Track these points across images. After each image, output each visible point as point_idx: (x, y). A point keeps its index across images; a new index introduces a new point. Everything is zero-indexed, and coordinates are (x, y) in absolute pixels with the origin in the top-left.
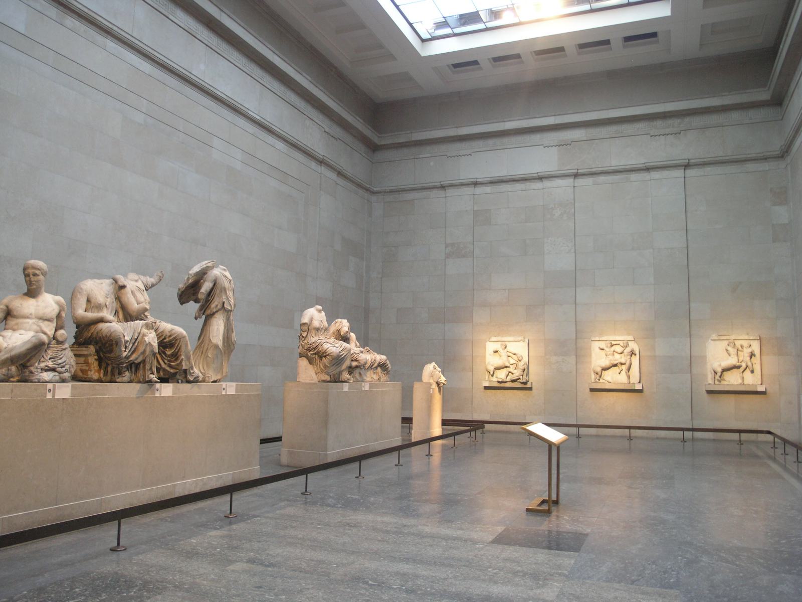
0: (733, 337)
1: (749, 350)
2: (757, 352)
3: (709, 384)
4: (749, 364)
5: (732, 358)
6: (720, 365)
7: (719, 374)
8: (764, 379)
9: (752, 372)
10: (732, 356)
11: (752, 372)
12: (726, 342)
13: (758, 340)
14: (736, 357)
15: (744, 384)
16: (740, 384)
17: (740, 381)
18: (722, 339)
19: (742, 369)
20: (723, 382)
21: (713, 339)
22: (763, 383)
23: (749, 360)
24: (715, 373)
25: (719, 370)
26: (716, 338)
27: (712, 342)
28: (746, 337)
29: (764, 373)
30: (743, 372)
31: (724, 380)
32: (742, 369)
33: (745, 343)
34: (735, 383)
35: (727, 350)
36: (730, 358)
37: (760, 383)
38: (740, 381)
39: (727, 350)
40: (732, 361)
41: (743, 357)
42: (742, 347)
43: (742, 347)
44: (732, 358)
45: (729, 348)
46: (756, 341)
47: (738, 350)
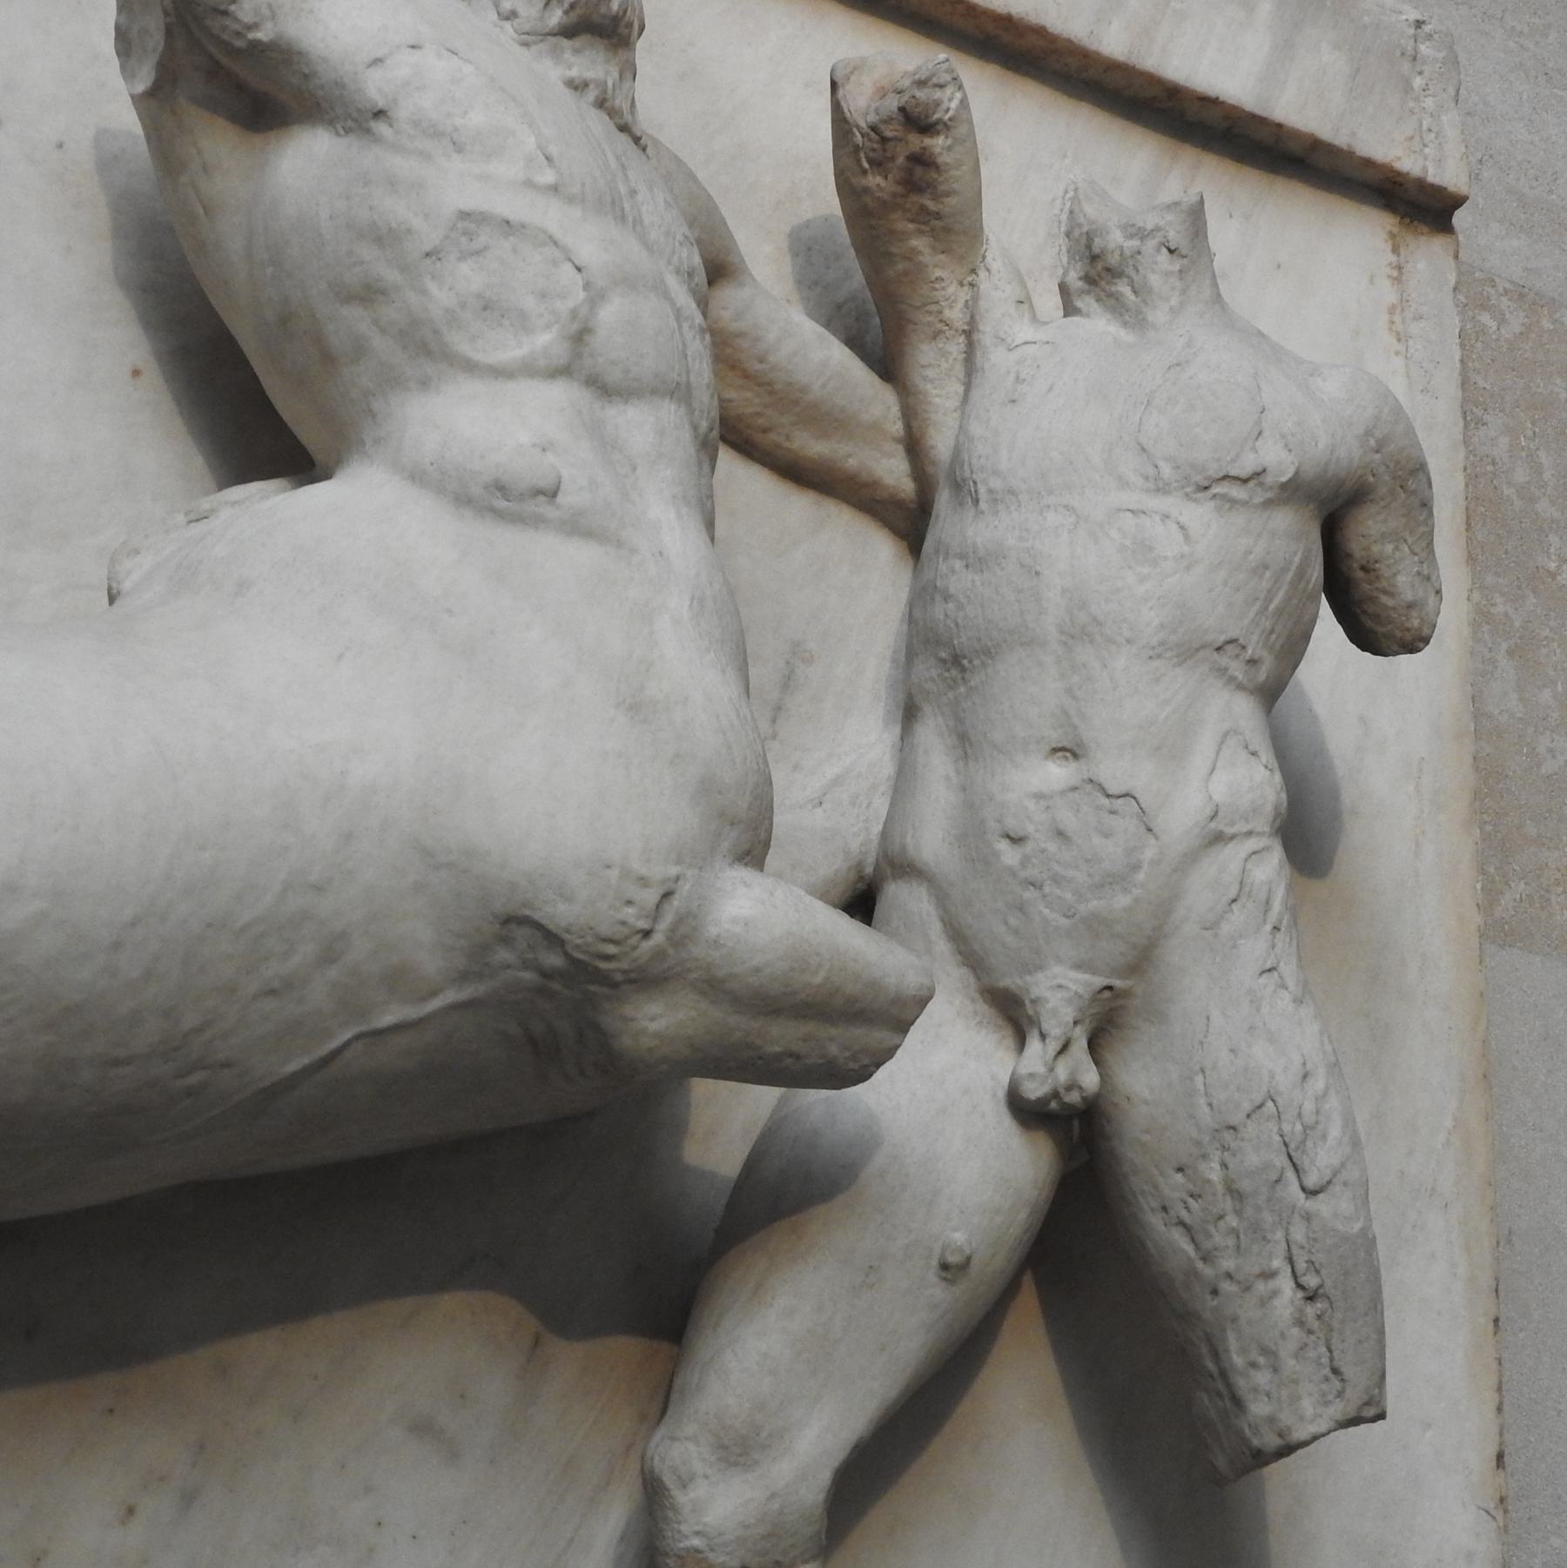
5: (510, 501)
44: (510, 501)
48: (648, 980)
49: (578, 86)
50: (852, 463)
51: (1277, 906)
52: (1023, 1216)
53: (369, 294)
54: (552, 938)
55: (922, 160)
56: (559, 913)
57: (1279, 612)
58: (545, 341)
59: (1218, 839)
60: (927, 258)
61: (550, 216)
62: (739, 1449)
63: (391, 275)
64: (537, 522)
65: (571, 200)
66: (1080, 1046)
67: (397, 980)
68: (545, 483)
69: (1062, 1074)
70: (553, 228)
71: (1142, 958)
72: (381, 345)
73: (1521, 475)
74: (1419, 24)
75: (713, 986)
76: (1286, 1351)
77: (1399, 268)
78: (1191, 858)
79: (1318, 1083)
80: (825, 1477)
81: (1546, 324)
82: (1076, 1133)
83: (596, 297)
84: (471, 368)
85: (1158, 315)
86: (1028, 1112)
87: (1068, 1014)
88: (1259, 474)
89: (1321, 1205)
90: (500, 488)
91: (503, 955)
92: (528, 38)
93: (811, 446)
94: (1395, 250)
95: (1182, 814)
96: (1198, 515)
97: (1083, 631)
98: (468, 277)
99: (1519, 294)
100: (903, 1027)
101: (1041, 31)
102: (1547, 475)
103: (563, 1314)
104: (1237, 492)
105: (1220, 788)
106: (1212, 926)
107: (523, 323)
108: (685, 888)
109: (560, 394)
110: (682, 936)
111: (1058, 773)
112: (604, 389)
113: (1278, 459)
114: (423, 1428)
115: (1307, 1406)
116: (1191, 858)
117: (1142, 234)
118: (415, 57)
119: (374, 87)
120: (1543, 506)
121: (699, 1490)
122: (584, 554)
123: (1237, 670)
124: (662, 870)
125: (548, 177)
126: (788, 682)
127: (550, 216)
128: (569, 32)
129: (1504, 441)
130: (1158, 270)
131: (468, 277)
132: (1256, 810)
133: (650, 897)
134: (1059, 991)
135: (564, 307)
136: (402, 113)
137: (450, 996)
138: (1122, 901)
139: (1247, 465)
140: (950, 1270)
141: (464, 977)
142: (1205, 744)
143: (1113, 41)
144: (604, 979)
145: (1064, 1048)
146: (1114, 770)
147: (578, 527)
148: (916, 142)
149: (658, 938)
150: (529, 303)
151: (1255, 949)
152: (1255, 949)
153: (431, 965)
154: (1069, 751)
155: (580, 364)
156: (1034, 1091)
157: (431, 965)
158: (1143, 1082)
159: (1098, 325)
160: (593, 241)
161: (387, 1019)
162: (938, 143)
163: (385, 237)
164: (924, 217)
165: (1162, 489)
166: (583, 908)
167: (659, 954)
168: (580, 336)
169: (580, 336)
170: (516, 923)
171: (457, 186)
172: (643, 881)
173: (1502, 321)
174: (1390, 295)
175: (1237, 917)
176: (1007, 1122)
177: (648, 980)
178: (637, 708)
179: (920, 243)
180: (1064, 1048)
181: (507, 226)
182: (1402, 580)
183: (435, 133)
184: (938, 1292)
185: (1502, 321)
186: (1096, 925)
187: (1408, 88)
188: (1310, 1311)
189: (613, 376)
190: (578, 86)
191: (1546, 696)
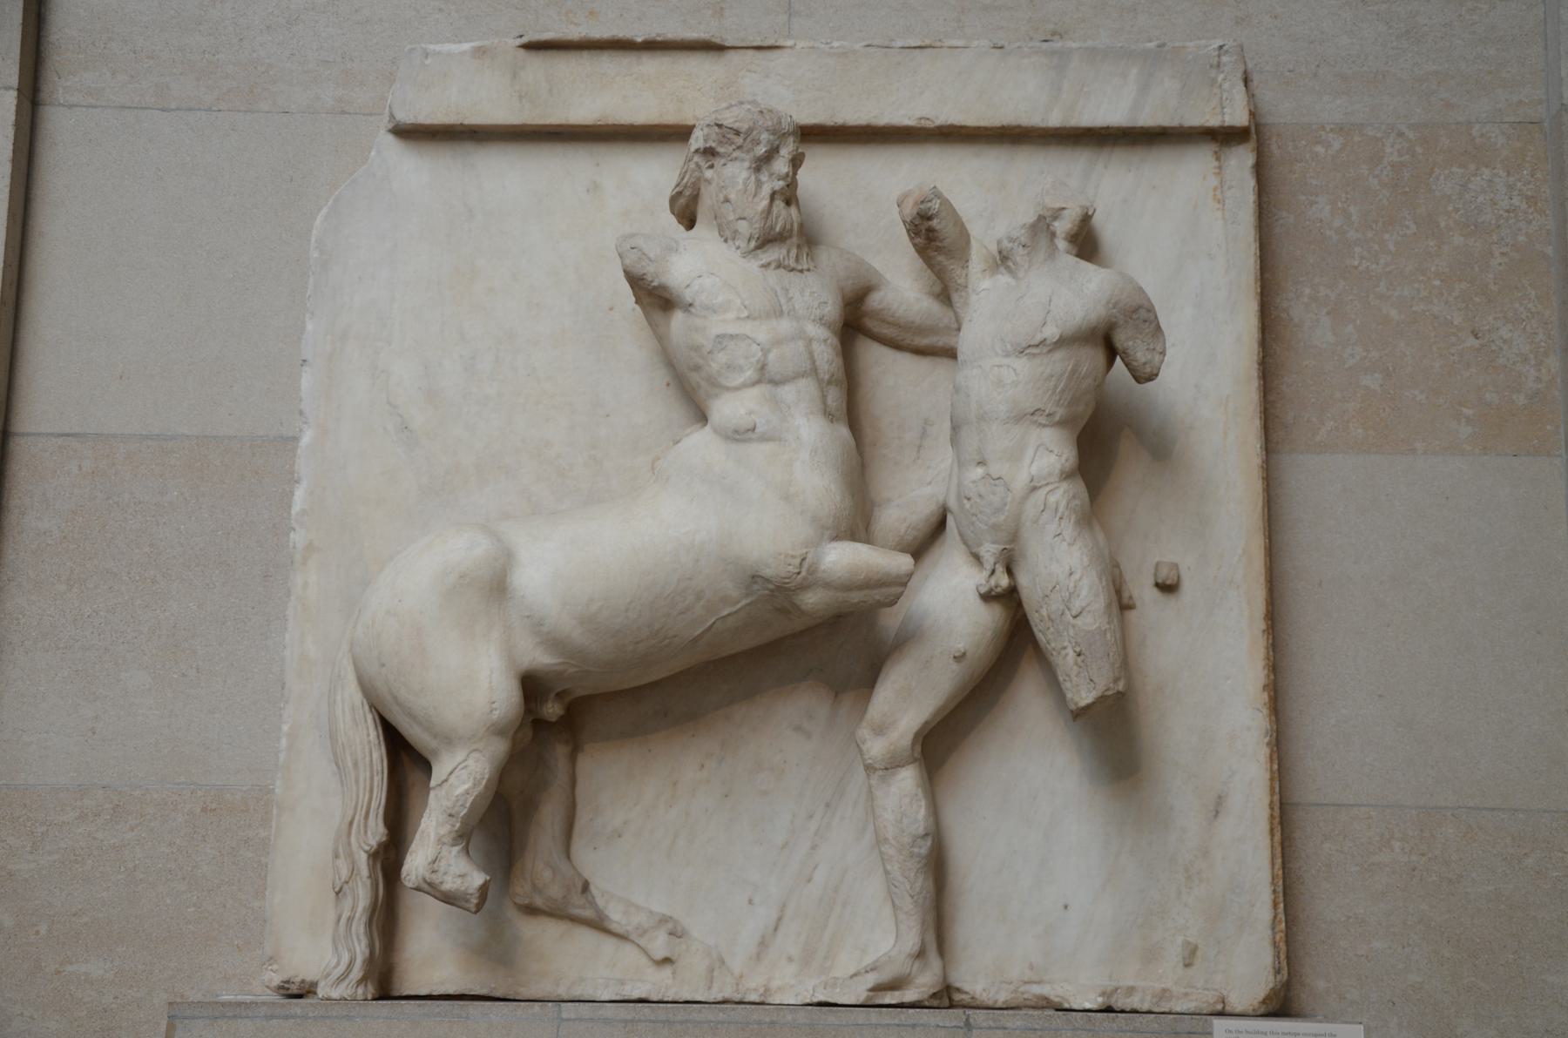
0: (790, 90)
1: (1073, 294)
2: (1203, 374)
3: (299, 992)
4: (1061, 569)
5: (740, 435)
6: (495, 586)
7: (459, 778)
8: (1332, 905)
9: (1114, 734)
10: (729, 408)
11: (1114, 734)
12: (654, 175)
13: (1225, 137)
14: (809, 434)
15: (946, 997)
16: (883, 997)
17: (879, 938)
18: (582, 112)
19: (905, 701)
20: (571, 961)
21: (406, 117)
22: (1317, 981)
23: (1063, 495)
24: (405, 759)
25: (466, 689)
26: (492, 103)
27: (414, 170)
28: (1023, 97)
29: (1327, 774)
30: (939, 745)
31: (579, 911)
32: (905, 701)
33: (990, 197)
34: (792, 985)
35: (656, 299)
36: (700, 444)
37: (1248, 970)
38: (879, 938)
39: (656, 299)
40: (732, 502)
41: (943, 457)
42: (931, 234)
43: (931, 234)
44: (740, 435)
45: (702, 264)
46: (1192, 171)
47: (856, 322)
48: (804, 587)
49: (765, 266)
50: (941, 344)
51: (1061, 509)
52: (989, 634)
53: (697, 368)
54: (768, 580)
55: (930, 230)
56: (768, 572)
57: (1063, 391)
58: (749, 374)
59: (1034, 489)
60: (946, 263)
61: (747, 328)
62: (880, 730)
63: (701, 362)
64: (749, 440)
65: (755, 319)
66: (1000, 569)
67: (725, 600)
68: (750, 426)
69: (993, 582)
70: (748, 333)
71: (1014, 537)
72: (703, 384)
73: (1337, 223)
74: (1221, 47)
75: (827, 585)
76: (1073, 674)
77: (1220, 168)
78: (1025, 498)
79: (1077, 576)
80: (911, 736)
81: (1357, 139)
82: (1009, 599)
83: (766, 352)
84: (728, 389)
85: (1021, 274)
86: (987, 597)
87: (992, 561)
88: (1043, 342)
89: (1079, 622)
90: (736, 432)
91: (756, 587)
92: (746, 254)
93: (924, 342)
94: (1218, 159)
95: (1020, 481)
96: (1021, 365)
97: (982, 418)
98: (722, 358)
99: (1340, 129)
100: (905, 585)
101: (1019, 127)
102: (1354, 218)
103: (837, 689)
104: (1035, 351)
105: (1034, 470)
106: (1036, 522)
107: (741, 369)
108: (810, 556)
109: (755, 391)
110: (813, 570)
111: (980, 471)
112: (775, 383)
113: (1052, 332)
114: (798, 729)
115: (1084, 694)
116: (1025, 498)
117: (1011, 240)
118: (700, 281)
119: (688, 296)
120: (1352, 235)
121: (869, 744)
122: (766, 447)
123: (1042, 420)
124: (801, 551)
125: (746, 313)
126: (924, 435)
127: (747, 328)
128: (758, 248)
129: (1328, 208)
130: (1063, 226)
131: (722, 358)
132: (1050, 474)
133: (797, 561)
134: (989, 551)
135: (753, 360)
136: (697, 303)
137: (744, 602)
138: (1002, 517)
139: (1038, 338)
140: (959, 658)
141: (747, 595)
142: (1030, 452)
143: (1054, 120)
144: (787, 589)
145: (993, 572)
146: (996, 469)
147: (764, 439)
148: (927, 224)
149: (804, 573)
150: (742, 362)
151: (1052, 528)
152: (1052, 528)
153: (735, 594)
154: (981, 463)
155: (764, 376)
156: (983, 590)
157: (735, 594)
158: (1023, 580)
159: (1004, 279)
160: (762, 332)
161: (725, 613)
162: (934, 223)
163: (697, 349)
164: (938, 249)
165: (1007, 355)
166: (775, 569)
167: (805, 579)
168: (763, 368)
169: (763, 368)
170: (755, 577)
171: (718, 325)
172: (793, 557)
173: (1328, 146)
174: (1214, 182)
175: (1045, 516)
176: (978, 601)
177: (804, 587)
178: (787, 498)
179: (940, 258)
180: (993, 572)
181: (732, 337)
182: (1139, 355)
183: (707, 308)
184: (955, 666)
185: (1328, 146)
186: (995, 527)
187: (1214, 81)
188: (1079, 659)
189: (778, 377)
190: (765, 266)
191: (1350, 328)
